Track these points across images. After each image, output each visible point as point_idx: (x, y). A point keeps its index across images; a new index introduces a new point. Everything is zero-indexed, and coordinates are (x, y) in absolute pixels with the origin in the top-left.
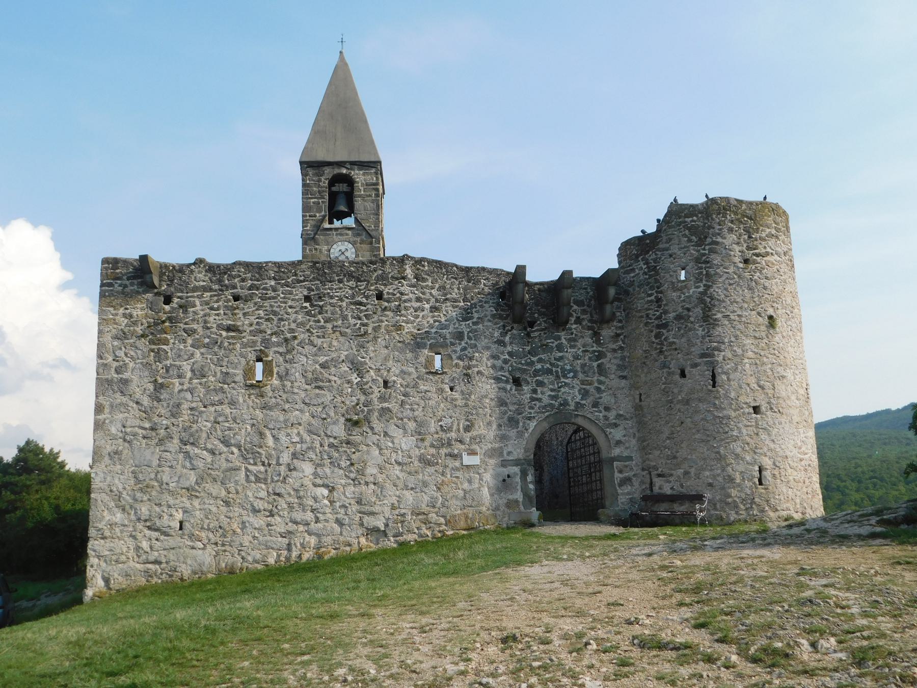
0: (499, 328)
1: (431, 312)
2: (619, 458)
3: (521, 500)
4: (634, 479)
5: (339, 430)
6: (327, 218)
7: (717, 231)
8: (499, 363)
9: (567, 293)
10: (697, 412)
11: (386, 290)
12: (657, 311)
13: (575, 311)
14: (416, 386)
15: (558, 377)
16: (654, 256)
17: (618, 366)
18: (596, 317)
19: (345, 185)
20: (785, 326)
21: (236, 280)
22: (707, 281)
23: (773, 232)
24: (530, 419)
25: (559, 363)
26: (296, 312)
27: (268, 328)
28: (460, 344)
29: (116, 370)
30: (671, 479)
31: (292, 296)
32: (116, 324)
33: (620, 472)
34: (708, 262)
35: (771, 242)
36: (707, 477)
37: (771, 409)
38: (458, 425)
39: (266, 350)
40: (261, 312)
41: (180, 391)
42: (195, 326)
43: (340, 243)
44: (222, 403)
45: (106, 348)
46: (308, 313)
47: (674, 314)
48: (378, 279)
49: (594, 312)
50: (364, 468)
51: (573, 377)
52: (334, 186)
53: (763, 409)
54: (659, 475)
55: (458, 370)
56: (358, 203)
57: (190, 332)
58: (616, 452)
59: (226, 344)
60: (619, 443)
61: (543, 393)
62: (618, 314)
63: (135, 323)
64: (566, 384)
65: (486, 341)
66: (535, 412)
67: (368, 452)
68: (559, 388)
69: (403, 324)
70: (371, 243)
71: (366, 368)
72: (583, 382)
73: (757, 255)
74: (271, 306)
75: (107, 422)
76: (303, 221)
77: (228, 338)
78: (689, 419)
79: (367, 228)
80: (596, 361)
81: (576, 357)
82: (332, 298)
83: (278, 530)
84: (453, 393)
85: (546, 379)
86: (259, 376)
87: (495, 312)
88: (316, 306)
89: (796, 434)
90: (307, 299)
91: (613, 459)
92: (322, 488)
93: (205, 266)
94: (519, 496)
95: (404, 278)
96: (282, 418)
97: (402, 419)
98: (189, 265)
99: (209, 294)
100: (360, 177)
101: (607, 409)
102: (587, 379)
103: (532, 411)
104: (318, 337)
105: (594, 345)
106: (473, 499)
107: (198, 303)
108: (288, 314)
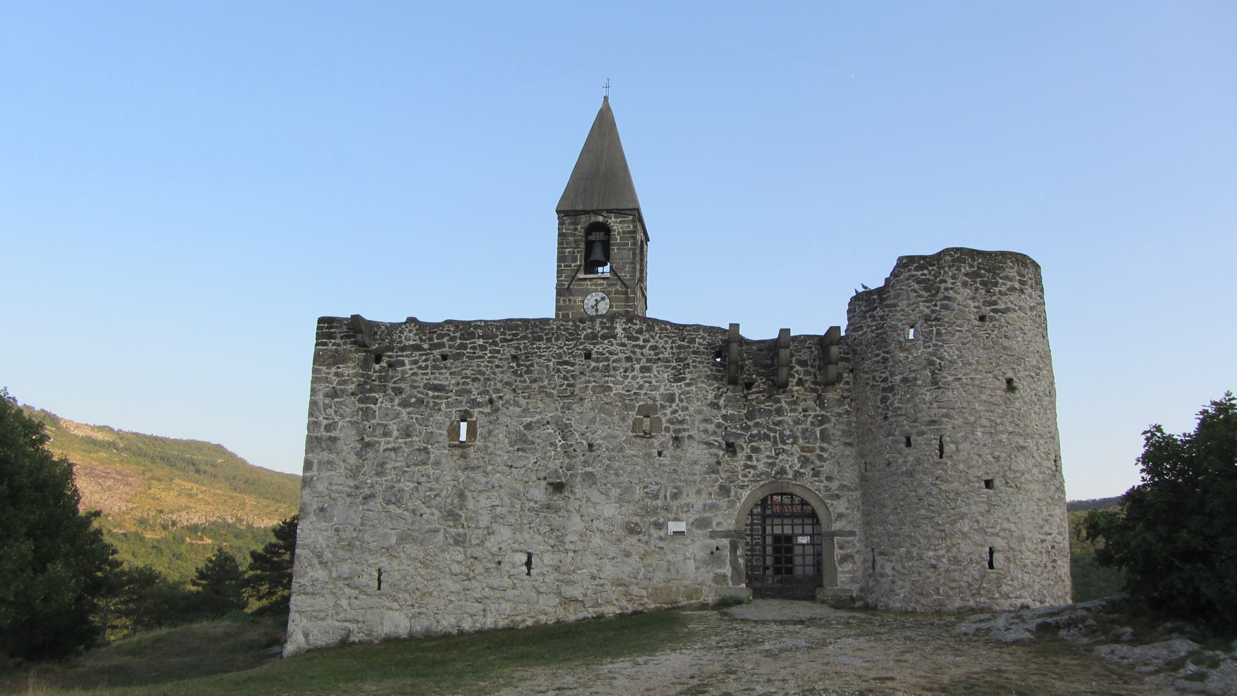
0: (713, 390)
1: (641, 372)
2: (841, 533)
3: (729, 575)
4: (857, 556)
5: (539, 493)
6: (582, 268)
7: (950, 286)
8: (711, 427)
9: (784, 353)
10: (921, 485)
11: (595, 350)
12: (884, 373)
13: (797, 372)
14: (621, 450)
15: (775, 443)
16: (881, 313)
17: (843, 431)
18: (819, 378)
19: (602, 233)
20: (1029, 390)
21: (445, 340)
22: (937, 340)
23: (1017, 285)
24: (742, 487)
25: (778, 428)
26: (502, 372)
27: (475, 389)
28: (670, 407)
29: (325, 427)
30: (894, 558)
31: (499, 356)
32: (328, 382)
33: (841, 548)
34: (939, 320)
35: (1013, 297)
36: (930, 558)
37: (1007, 483)
38: (666, 492)
39: (471, 410)
40: (468, 372)
41: (385, 450)
42: (403, 385)
43: (594, 294)
44: (425, 464)
45: (317, 406)
46: (515, 373)
47: (901, 376)
48: (587, 337)
49: (817, 373)
50: (564, 535)
51: (793, 443)
53: (997, 483)
54: (881, 554)
55: (668, 434)
56: (614, 250)
57: (399, 391)
58: (837, 526)
59: (431, 404)
60: (840, 516)
61: (758, 460)
62: (846, 375)
63: (345, 382)
64: (784, 450)
65: (699, 403)
66: (749, 481)
67: (569, 518)
68: (777, 454)
69: (611, 385)
70: (626, 293)
71: (570, 431)
72: (803, 449)
73: (995, 311)
74: (479, 366)
75: (315, 478)
76: (559, 272)
77: (434, 397)
78: (914, 493)
80: (819, 426)
81: (797, 422)
82: (540, 357)
83: (475, 595)
84: (661, 458)
85: (762, 445)
86: (463, 437)
87: (710, 373)
88: (522, 365)
89: (1037, 512)
90: (515, 358)
91: (834, 534)
92: (520, 553)
93: (415, 326)
94: (727, 570)
95: (615, 337)
96: (483, 480)
97: (606, 485)
98: (400, 324)
99: (418, 353)
100: (617, 225)
101: (829, 479)
102: (808, 445)
103: (746, 479)
104: (524, 397)
105: (818, 408)
106: (678, 572)
107: (407, 362)
108: (495, 374)
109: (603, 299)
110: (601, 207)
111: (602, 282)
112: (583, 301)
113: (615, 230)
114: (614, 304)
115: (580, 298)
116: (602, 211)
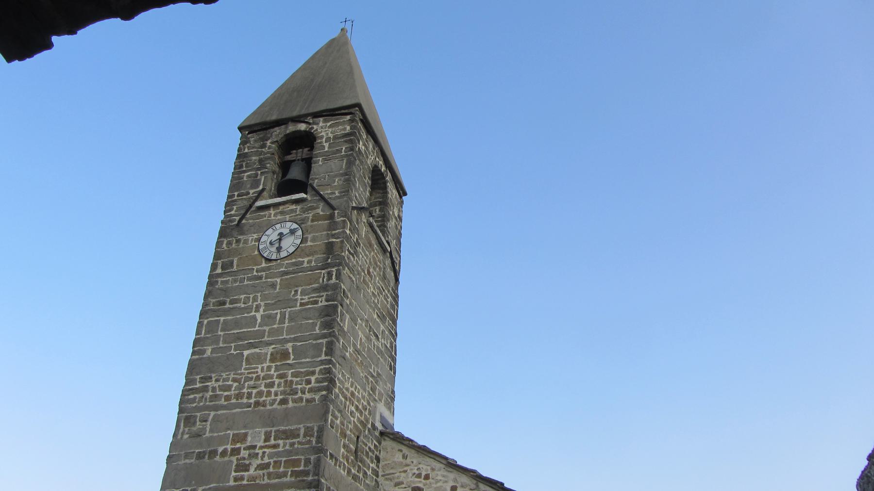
43: (278, 226)
52: (291, 154)
70: (331, 217)
79: (326, 197)
109: (292, 232)
110: (303, 112)
111: (294, 207)
112: (259, 240)
113: (322, 137)
114: (310, 236)
115: (255, 236)
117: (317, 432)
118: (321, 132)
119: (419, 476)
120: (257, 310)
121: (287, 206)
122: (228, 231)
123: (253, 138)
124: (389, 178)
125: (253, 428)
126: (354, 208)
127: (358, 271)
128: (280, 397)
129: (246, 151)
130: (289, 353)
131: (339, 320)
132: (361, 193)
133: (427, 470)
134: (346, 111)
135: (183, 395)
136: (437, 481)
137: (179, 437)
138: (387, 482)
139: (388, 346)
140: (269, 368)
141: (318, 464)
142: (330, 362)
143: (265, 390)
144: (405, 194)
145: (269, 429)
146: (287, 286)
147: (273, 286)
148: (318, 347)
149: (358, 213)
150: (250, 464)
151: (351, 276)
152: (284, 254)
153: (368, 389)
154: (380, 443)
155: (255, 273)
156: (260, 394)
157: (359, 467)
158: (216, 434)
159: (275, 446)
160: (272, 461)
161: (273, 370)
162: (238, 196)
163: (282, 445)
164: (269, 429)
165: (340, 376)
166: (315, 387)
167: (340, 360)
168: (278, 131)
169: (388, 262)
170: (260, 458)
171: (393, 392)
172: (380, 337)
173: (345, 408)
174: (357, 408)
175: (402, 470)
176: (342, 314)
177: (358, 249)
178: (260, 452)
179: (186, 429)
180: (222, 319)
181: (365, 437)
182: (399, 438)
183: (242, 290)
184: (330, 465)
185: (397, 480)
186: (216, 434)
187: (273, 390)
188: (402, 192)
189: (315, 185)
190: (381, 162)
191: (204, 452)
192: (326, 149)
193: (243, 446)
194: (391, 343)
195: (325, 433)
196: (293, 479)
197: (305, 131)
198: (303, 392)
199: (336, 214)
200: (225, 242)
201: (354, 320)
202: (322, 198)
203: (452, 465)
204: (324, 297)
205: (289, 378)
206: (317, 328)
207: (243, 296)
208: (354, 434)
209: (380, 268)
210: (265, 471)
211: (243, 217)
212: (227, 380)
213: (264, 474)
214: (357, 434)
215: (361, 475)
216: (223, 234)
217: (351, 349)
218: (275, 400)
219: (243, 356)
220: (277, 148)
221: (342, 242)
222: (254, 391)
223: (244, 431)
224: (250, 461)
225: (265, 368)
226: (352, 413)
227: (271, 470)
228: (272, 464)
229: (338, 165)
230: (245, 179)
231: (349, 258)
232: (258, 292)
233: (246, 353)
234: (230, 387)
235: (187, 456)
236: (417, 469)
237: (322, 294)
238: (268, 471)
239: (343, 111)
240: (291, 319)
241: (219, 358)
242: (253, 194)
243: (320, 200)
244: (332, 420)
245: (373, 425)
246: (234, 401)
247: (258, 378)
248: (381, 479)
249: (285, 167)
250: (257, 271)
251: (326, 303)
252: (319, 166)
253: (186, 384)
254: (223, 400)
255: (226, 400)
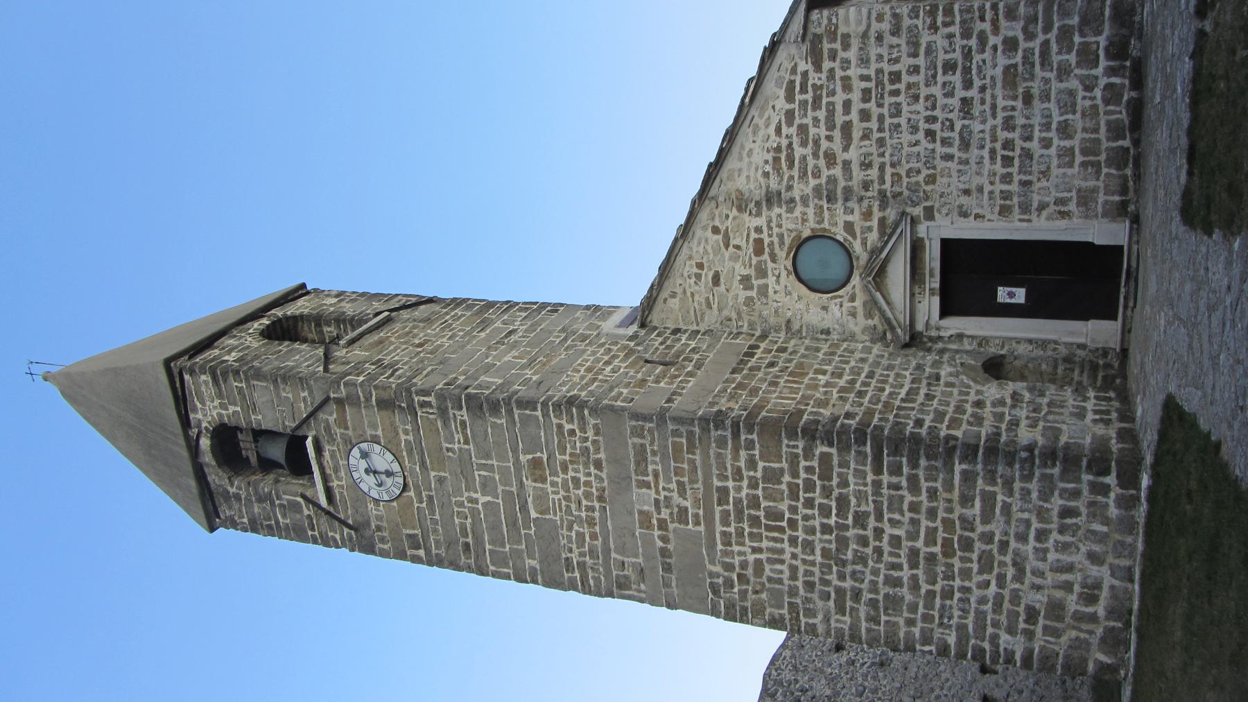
43: (356, 475)
52: (248, 458)
70: (339, 402)
79: (310, 409)
109: (365, 455)
110: (182, 441)
111: (327, 454)
112: (376, 501)
113: (220, 415)
114: (369, 432)
116: (187, 437)
117: (638, 421)
118: (212, 416)
119: (698, 276)
120: (476, 501)
121: (325, 463)
122: (364, 542)
123: (225, 512)
124: (278, 312)
125: (632, 503)
126: (326, 370)
127: (418, 363)
128: (592, 470)
129: (245, 520)
130: (533, 458)
131: (487, 392)
132: (303, 357)
133: (691, 266)
134: (177, 380)
135: (590, 593)
136: (706, 252)
137: (643, 595)
138: (706, 319)
139: (524, 314)
140: (554, 484)
141: (678, 420)
142: (545, 404)
143: (582, 489)
144: (303, 286)
145: (634, 483)
146: (440, 462)
147: (441, 480)
148: (525, 421)
149: (333, 362)
150: (678, 506)
151: (425, 372)
152: (396, 467)
153: (582, 346)
154: (655, 328)
155: (424, 505)
156: (588, 495)
157: (683, 360)
158: (640, 550)
159: (656, 475)
160: (674, 479)
161: (556, 479)
162: (313, 529)
163: (654, 467)
164: (634, 483)
165: (564, 389)
166: (579, 424)
167: (543, 388)
168: (213, 477)
169: (405, 314)
170: (671, 494)
171: (588, 307)
172: (512, 328)
173: (607, 381)
174: (608, 363)
175: (691, 299)
176: (480, 386)
177: (386, 362)
178: (663, 493)
179: (634, 587)
180: (488, 547)
181: (646, 350)
182: (650, 302)
183: (447, 522)
184: (681, 402)
185: (704, 306)
186: (640, 550)
187: (583, 479)
188: (300, 291)
189: (294, 425)
190: (256, 325)
191: (662, 564)
192: (239, 409)
193: (655, 515)
194: (521, 310)
195: (639, 411)
196: (698, 452)
197: (212, 438)
198: (586, 439)
199: (335, 395)
200: (381, 546)
201: (487, 369)
202: (312, 414)
203: (685, 231)
204: (455, 412)
205: (567, 458)
206: (499, 422)
207: (457, 521)
208: (642, 368)
209: (414, 327)
210: (688, 487)
211: (344, 523)
212: (569, 538)
213: (691, 489)
214: (642, 363)
215: (696, 357)
216: (369, 549)
217: (529, 372)
218: (596, 476)
219: (538, 518)
220: (240, 478)
221: (376, 387)
222: (584, 502)
223: (637, 515)
224: (675, 505)
225: (554, 489)
226: (613, 371)
227: (686, 479)
228: (678, 478)
229: (262, 393)
230: (288, 521)
231: (400, 377)
232: (450, 501)
233: (534, 515)
234: (578, 533)
235: (667, 585)
236: (690, 278)
237: (452, 416)
238: (687, 484)
239: (178, 384)
240: (488, 456)
241: (540, 550)
242: (309, 510)
243: (315, 419)
244: (622, 401)
245: (631, 338)
246: (597, 529)
247: (567, 498)
248: (702, 328)
249: (267, 465)
250: (421, 502)
251: (464, 409)
252: (264, 419)
253: (575, 589)
254: (596, 542)
255: (596, 539)
